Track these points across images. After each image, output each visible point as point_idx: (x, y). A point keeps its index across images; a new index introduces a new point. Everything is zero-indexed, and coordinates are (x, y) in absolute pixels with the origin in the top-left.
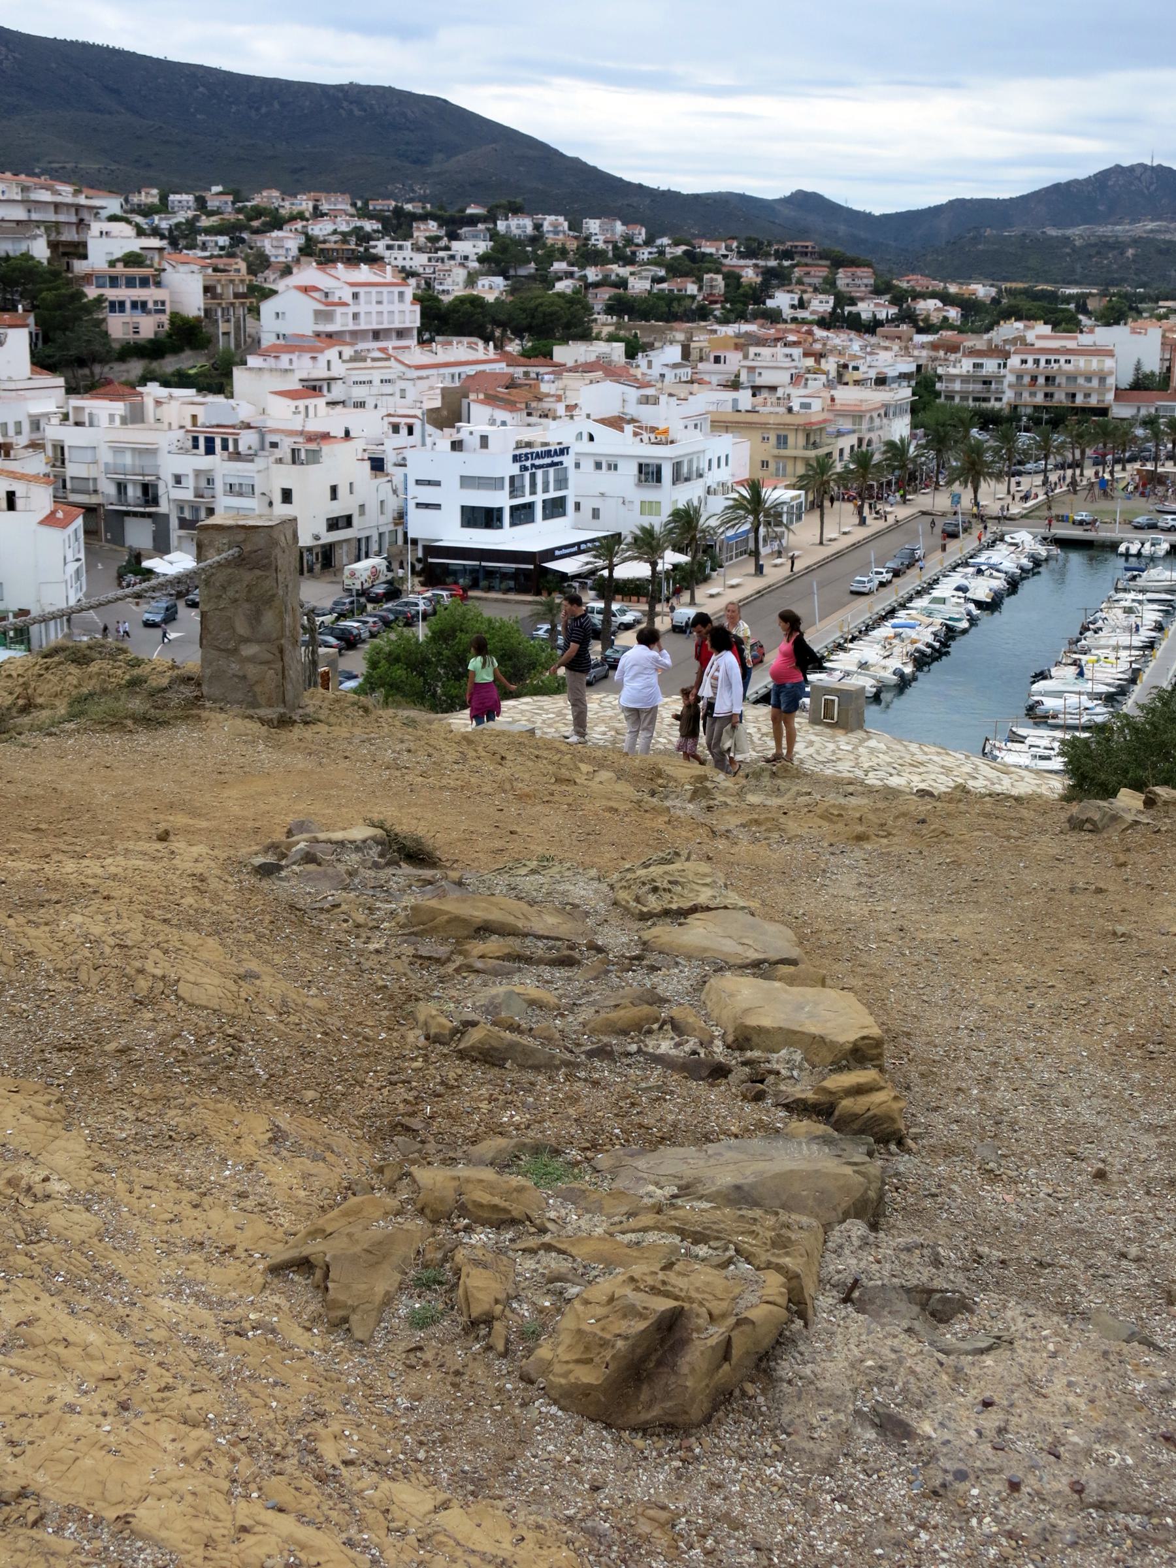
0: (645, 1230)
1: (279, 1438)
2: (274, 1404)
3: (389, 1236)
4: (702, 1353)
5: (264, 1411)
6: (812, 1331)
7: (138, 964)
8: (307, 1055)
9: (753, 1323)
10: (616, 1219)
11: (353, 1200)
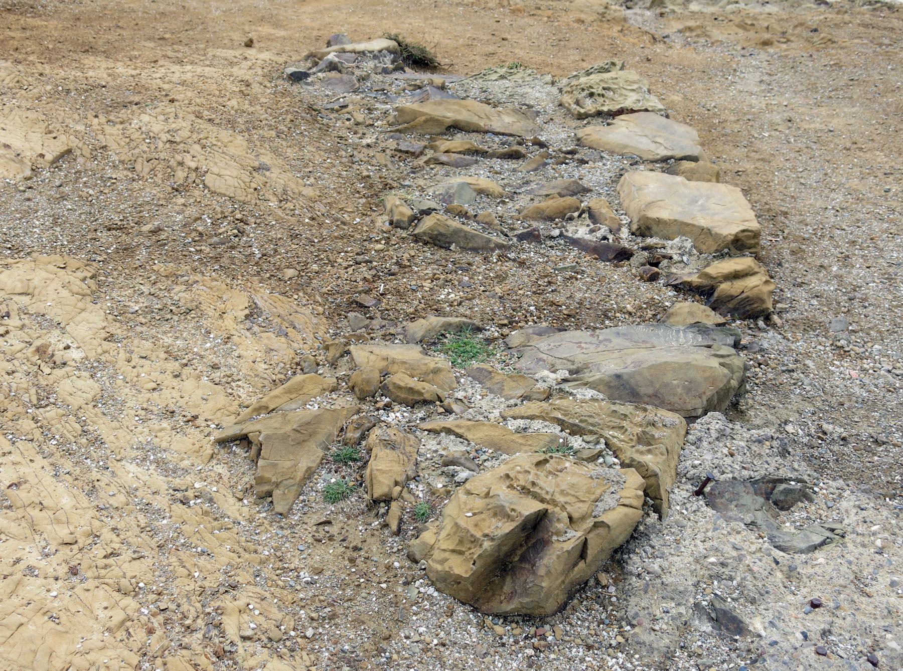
0: (532, 418)
1: (191, 609)
2: (196, 574)
3: (317, 416)
4: (558, 557)
5: (186, 581)
6: (666, 521)
7: (179, 158)
8: (294, 237)
9: (608, 527)
10: (512, 402)
11: (299, 377)
